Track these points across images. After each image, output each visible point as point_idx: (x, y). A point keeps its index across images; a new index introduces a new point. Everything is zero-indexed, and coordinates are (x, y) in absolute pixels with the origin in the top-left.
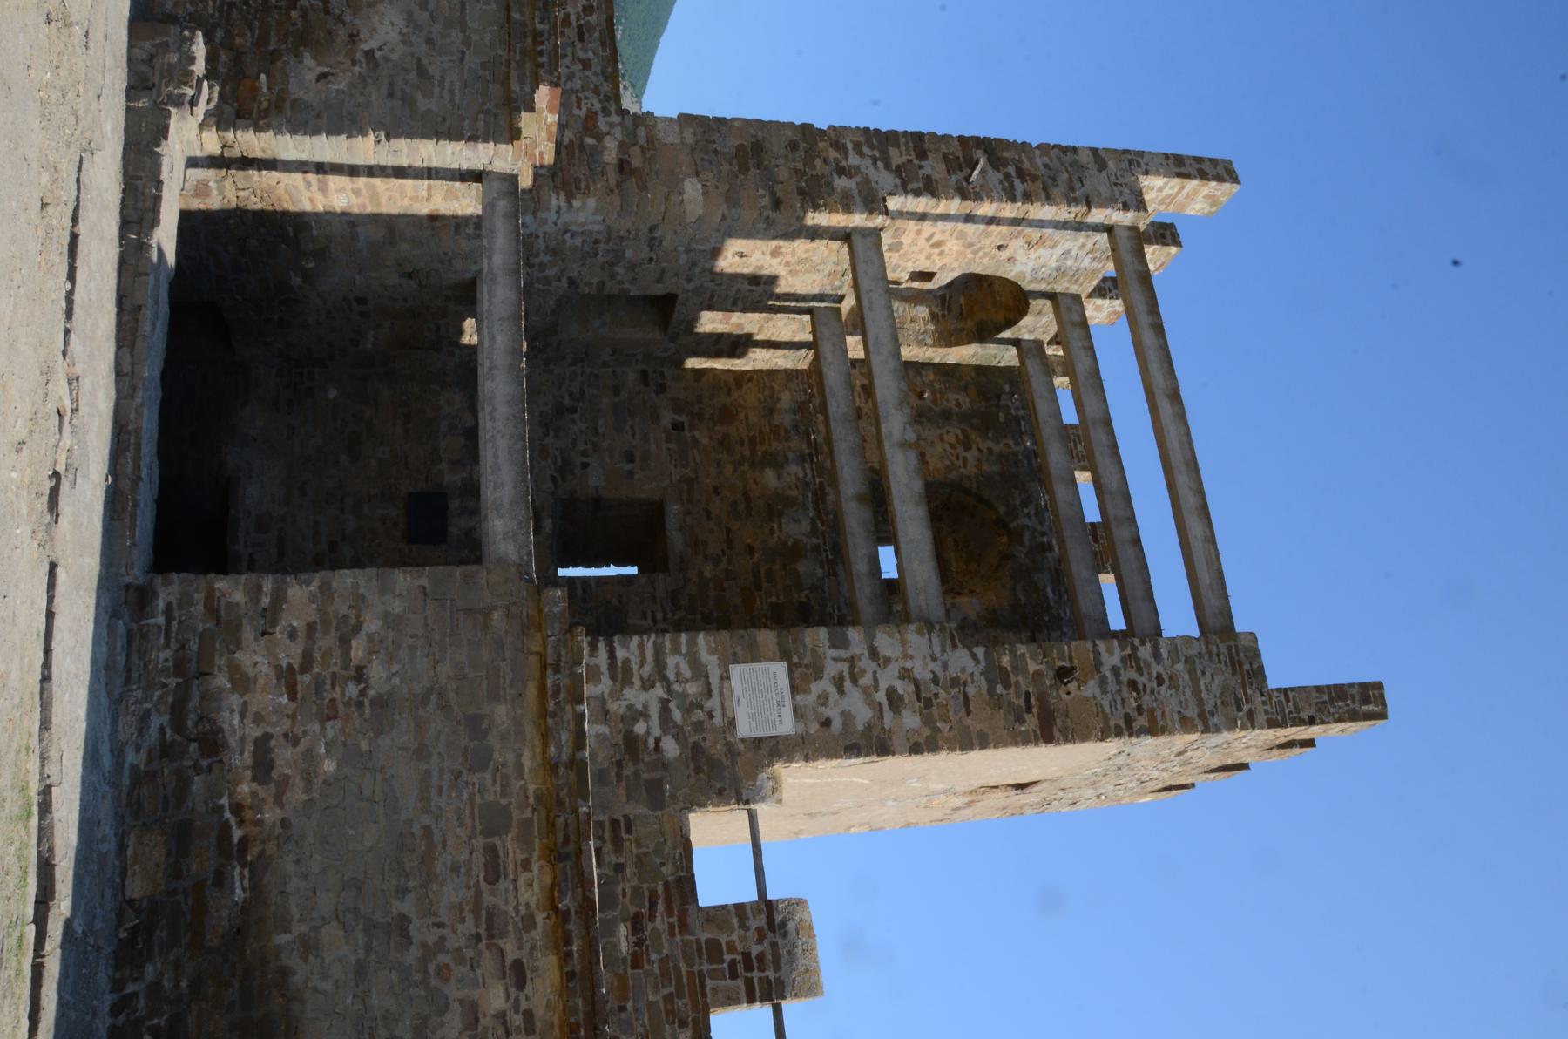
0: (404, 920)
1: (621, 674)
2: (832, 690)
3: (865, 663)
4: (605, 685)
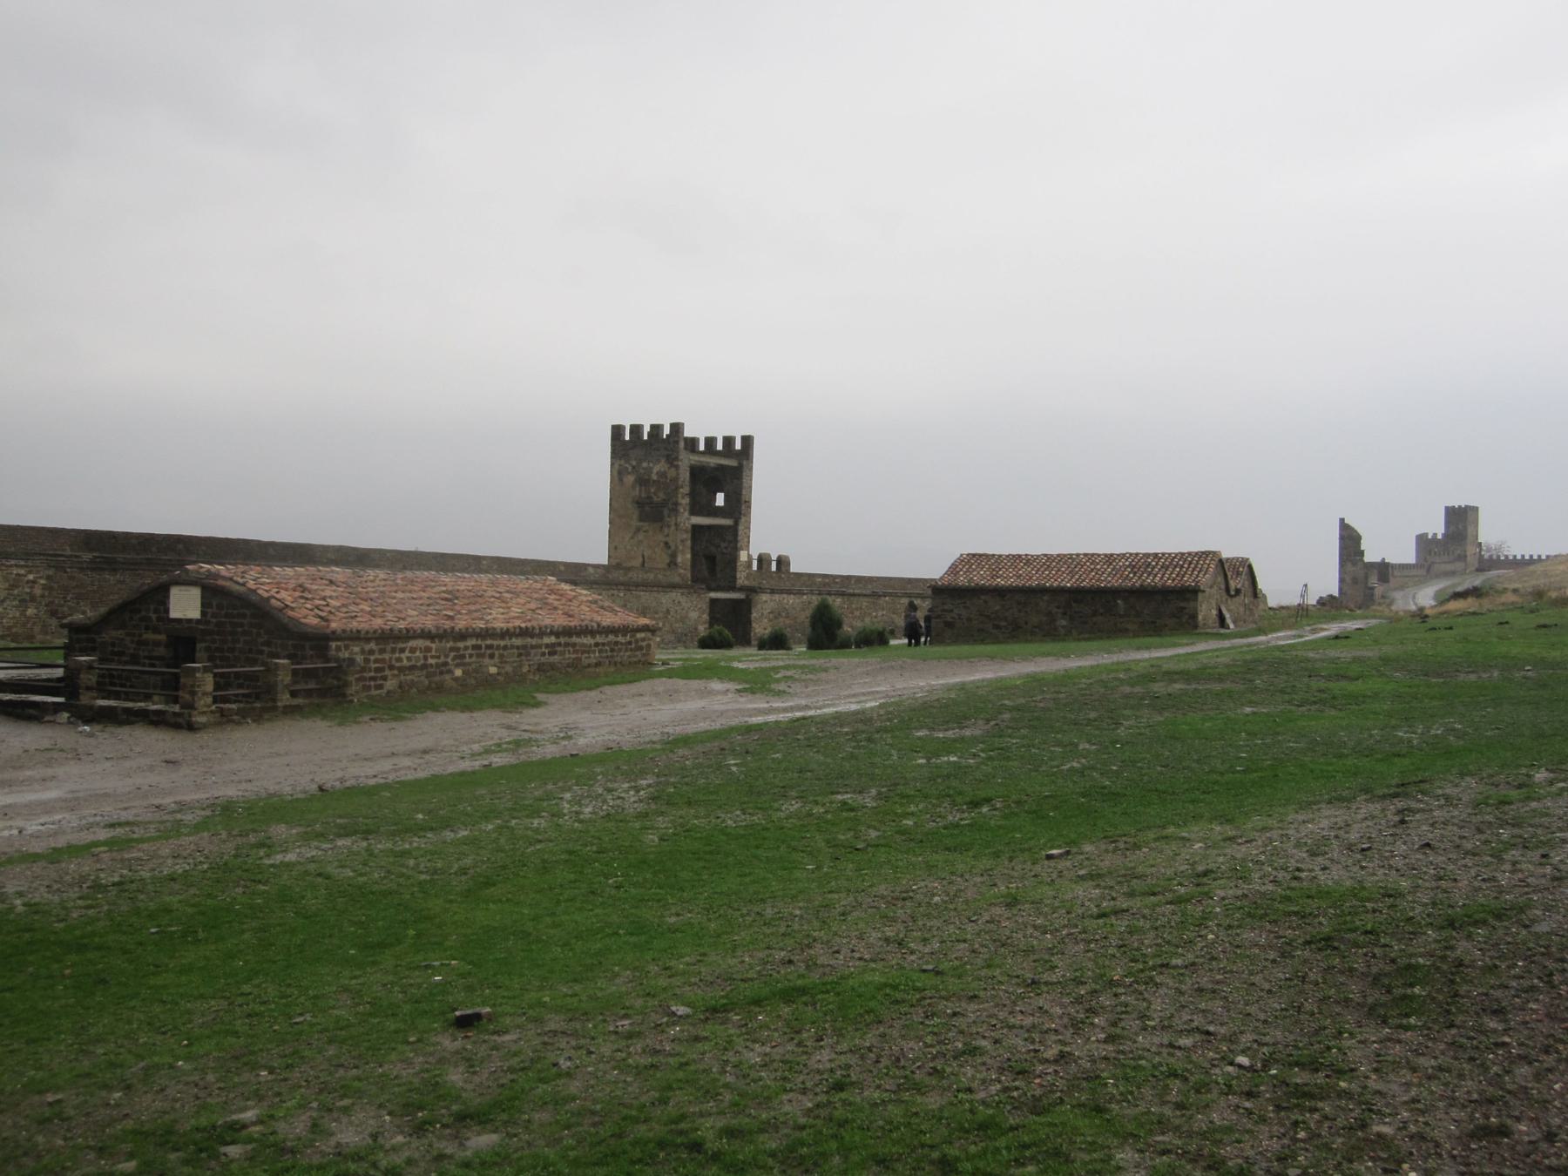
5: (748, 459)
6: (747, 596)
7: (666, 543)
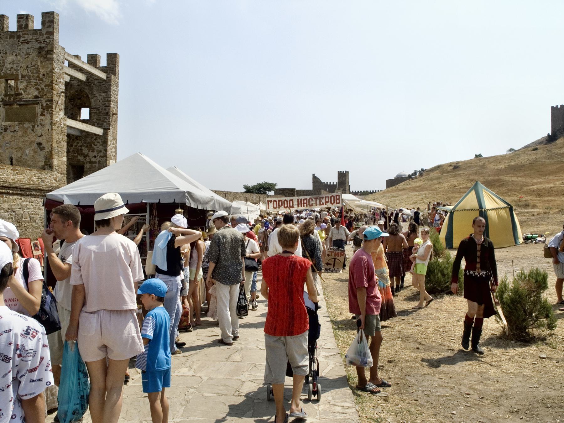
3: (110, 147)
5: (115, 75)
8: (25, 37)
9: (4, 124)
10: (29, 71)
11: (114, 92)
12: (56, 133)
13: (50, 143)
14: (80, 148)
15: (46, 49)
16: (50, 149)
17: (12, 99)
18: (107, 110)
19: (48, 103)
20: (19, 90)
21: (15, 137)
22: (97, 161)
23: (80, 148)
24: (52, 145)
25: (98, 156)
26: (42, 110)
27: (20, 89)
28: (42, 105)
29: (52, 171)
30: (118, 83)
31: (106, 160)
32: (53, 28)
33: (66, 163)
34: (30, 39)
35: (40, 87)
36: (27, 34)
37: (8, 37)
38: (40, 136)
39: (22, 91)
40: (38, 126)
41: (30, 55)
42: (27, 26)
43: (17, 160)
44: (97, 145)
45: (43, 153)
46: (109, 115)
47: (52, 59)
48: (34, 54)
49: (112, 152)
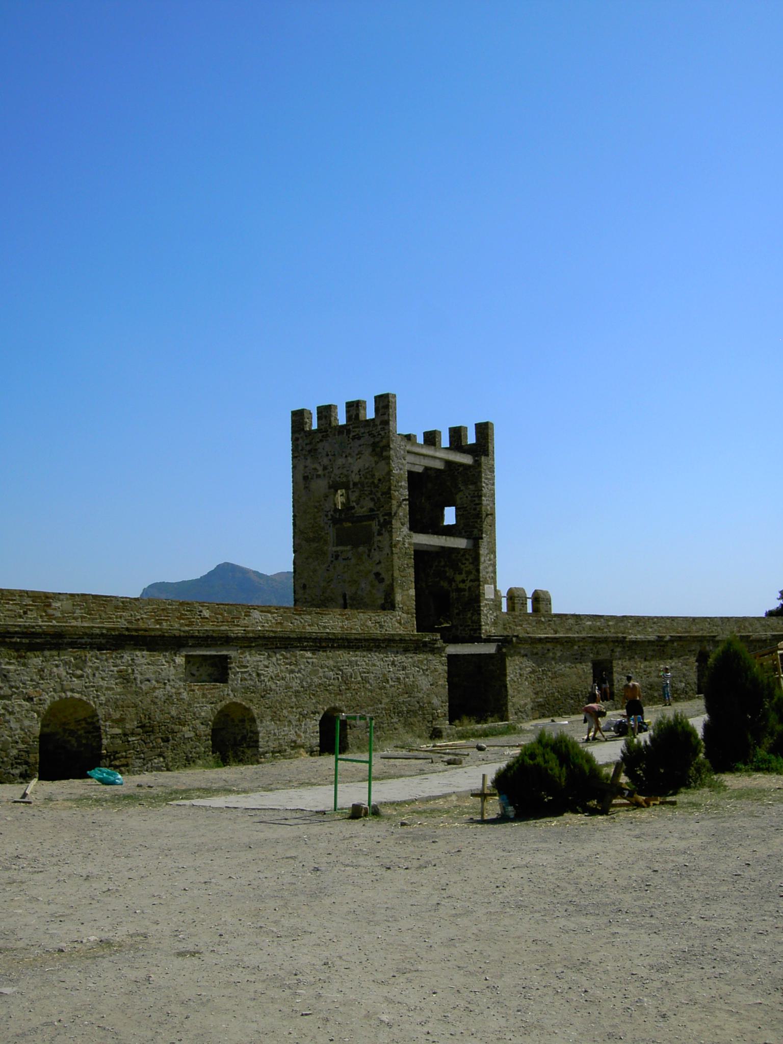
0: (542, 670)
1: (487, 624)
2: (488, 575)
3: (485, 565)
4: (487, 627)
5: (487, 455)
6: (499, 649)
7: (377, 575)
8: (355, 431)
9: (335, 549)
10: (361, 476)
11: (486, 481)
12: (398, 558)
13: (390, 573)
14: (442, 569)
15: (381, 444)
16: (391, 580)
17: (343, 515)
18: (478, 509)
19: (386, 517)
20: (351, 503)
21: (348, 566)
22: (467, 588)
23: (442, 569)
24: (392, 575)
25: (467, 580)
26: (378, 527)
27: (353, 502)
28: (379, 521)
29: (394, 610)
30: (493, 465)
31: (479, 585)
32: (389, 415)
33: (414, 598)
34: (363, 433)
35: (376, 496)
36: (357, 427)
37: (337, 433)
38: (378, 564)
39: (354, 504)
40: (375, 550)
41: (362, 454)
42: (357, 416)
43: (352, 599)
44: (465, 563)
45: (383, 587)
46: (481, 518)
47: (388, 458)
48: (367, 452)
49: (487, 573)
